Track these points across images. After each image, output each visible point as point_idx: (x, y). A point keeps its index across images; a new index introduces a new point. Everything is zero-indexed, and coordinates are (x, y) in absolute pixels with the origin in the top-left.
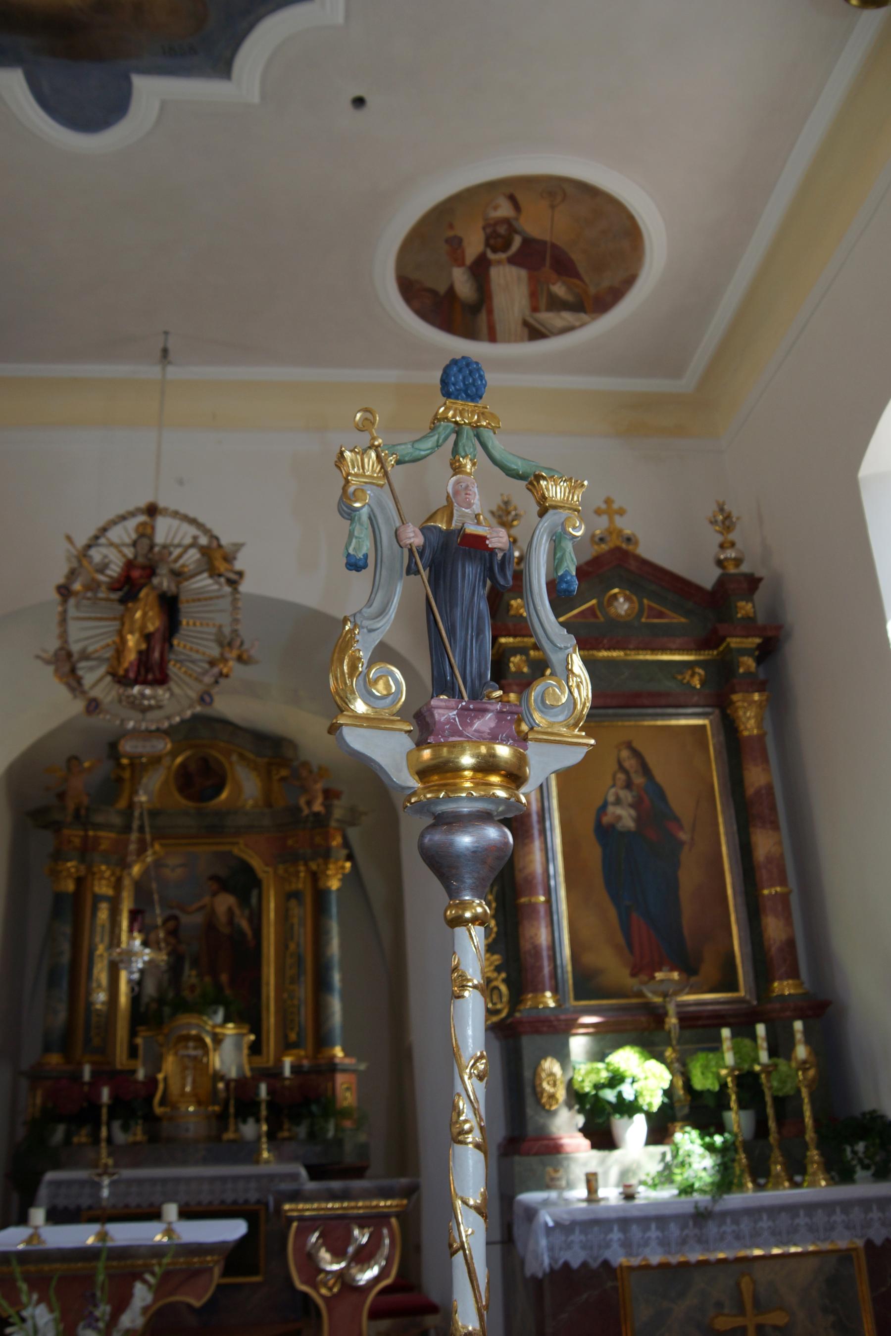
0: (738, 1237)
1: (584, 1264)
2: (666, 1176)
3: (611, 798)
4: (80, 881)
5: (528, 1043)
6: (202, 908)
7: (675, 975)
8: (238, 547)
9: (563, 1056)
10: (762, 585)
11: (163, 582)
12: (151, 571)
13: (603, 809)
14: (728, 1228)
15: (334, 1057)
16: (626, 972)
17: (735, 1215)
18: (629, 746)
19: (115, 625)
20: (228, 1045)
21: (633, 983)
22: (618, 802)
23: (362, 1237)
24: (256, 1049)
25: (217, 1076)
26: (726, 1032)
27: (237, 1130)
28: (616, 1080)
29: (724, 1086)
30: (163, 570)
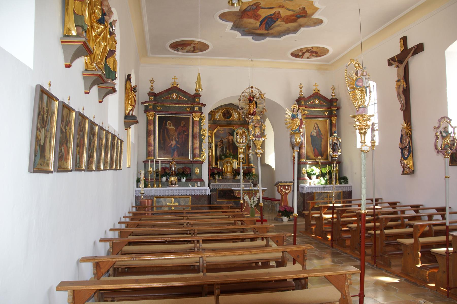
0: (328, 190)
1: (310, 192)
2: (319, 183)
3: (313, 131)
5: (301, 166)
6: (227, 138)
7: (320, 157)
8: (265, 94)
9: (306, 168)
10: (338, 100)
11: (256, 100)
12: (254, 97)
14: (327, 189)
15: (252, 166)
16: (314, 156)
17: (328, 187)
18: (316, 123)
19: (248, 105)
20: (234, 163)
21: (314, 158)
22: (314, 132)
23: (287, 187)
25: (233, 168)
26: (328, 165)
27: (237, 177)
28: (312, 171)
29: (327, 172)
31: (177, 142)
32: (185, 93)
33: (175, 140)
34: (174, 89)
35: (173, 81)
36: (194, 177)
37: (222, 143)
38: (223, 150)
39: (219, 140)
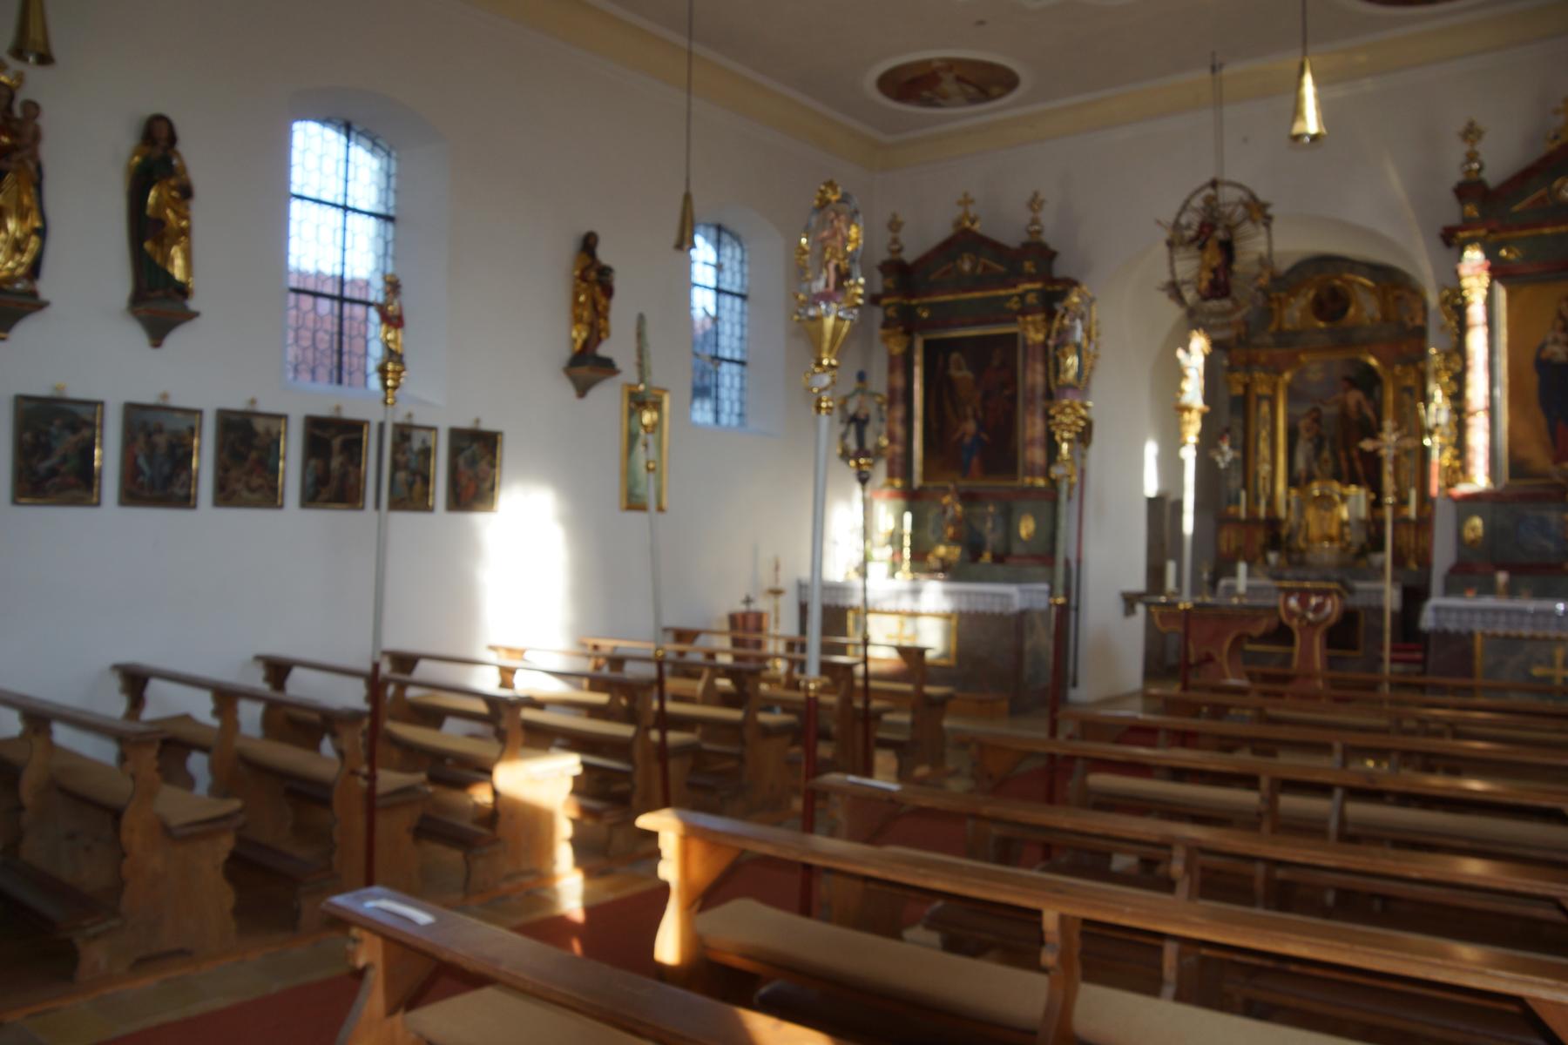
3: (1550, 339)
4: (1247, 387)
11: (1220, 234)
13: (1541, 348)
22: (1556, 341)
24: (1376, 504)
30: (1221, 225)
31: (982, 426)
32: (995, 248)
33: (975, 417)
34: (964, 240)
35: (959, 211)
36: (1017, 549)
37: (1317, 420)
38: (1318, 448)
39: (1305, 408)
